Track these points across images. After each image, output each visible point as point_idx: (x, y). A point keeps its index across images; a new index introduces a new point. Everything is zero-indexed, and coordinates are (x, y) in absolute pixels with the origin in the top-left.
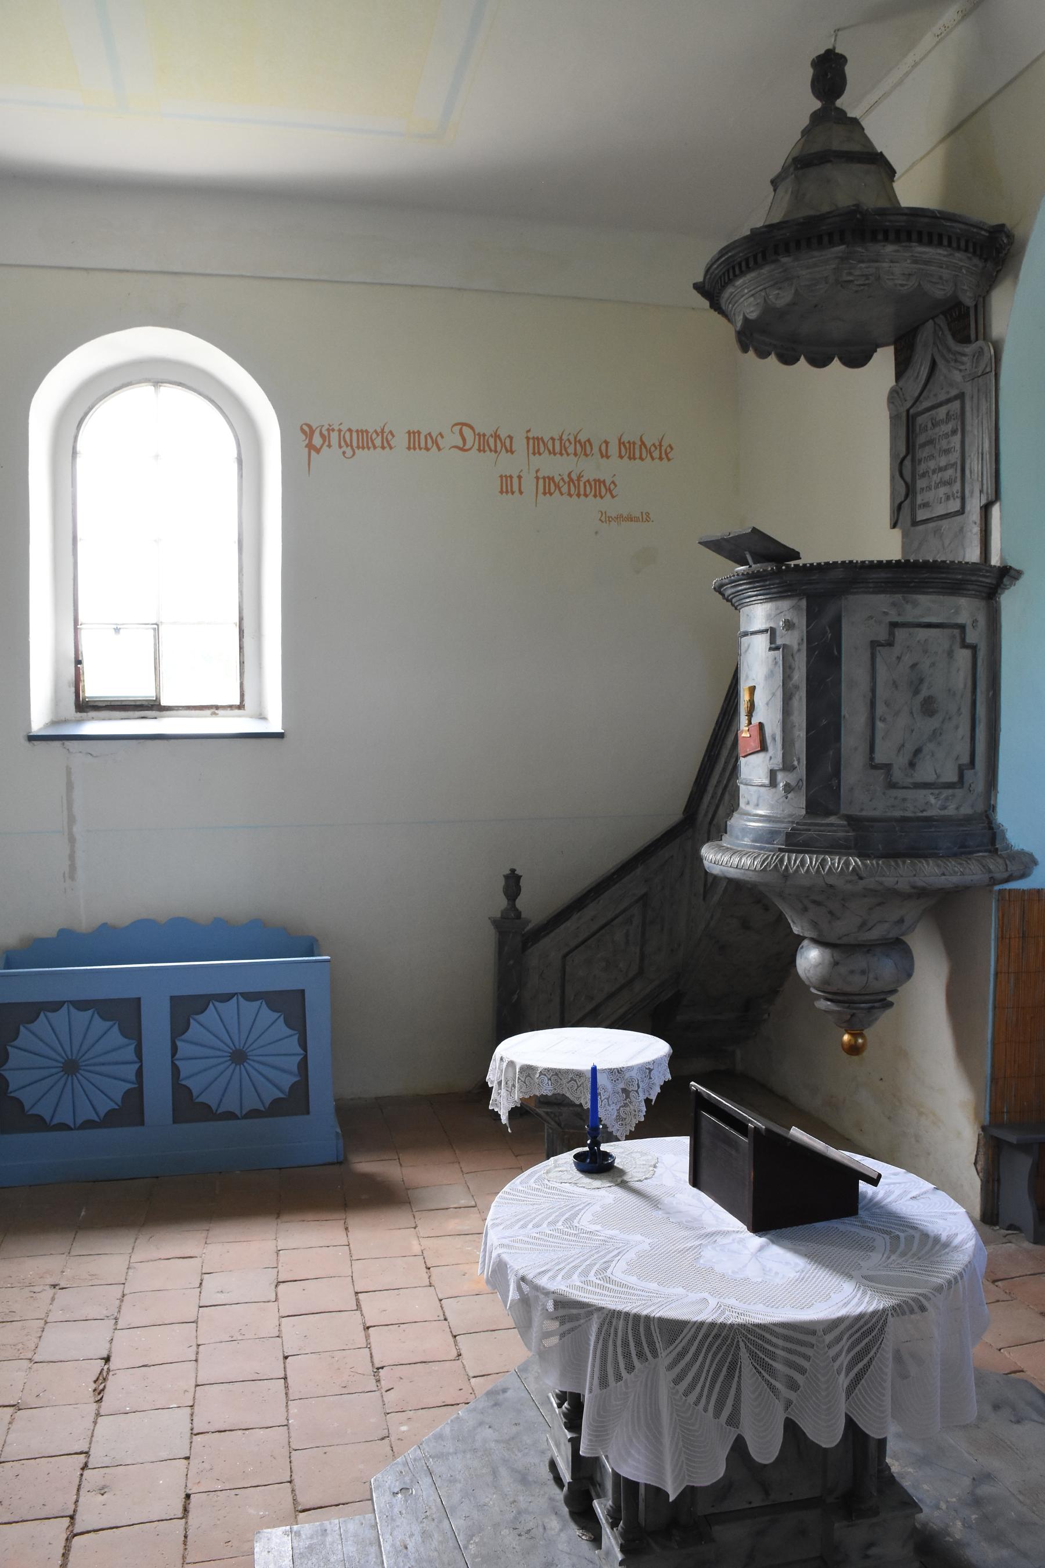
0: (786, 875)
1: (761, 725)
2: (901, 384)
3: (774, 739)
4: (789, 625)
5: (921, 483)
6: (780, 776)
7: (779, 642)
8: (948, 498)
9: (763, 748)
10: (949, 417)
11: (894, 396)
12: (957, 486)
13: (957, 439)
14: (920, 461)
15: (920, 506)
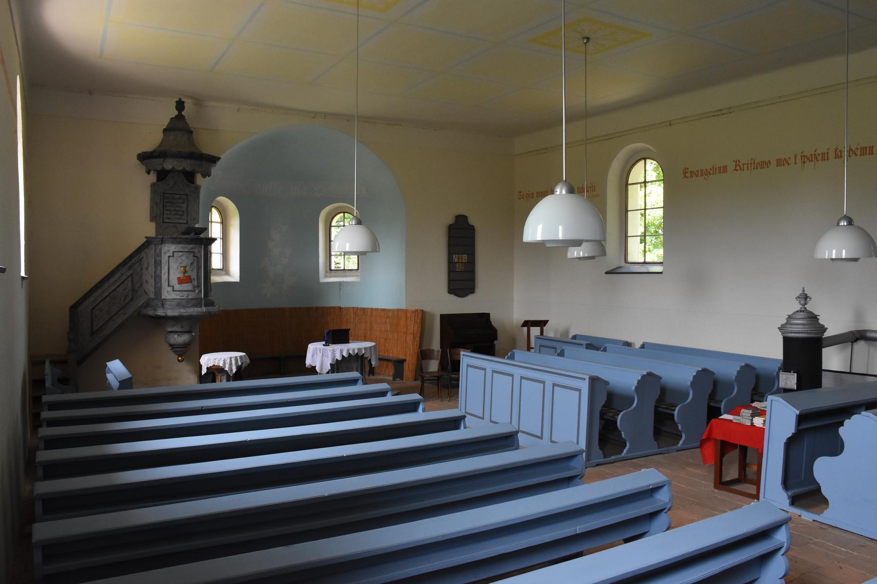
0: (210, 312)
1: (190, 276)
2: (158, 183)
3: (194, 279)
4: (199, 251)
5: (165, 212)
6: (196, 289)
7: (195, 255)
8: (180, 219)
9: (191, 282)
10: (180, 198)
11: (153, 185)
12: (185, 217)
13: (185, 204)
14: (166, 206)
15: (166, 218)
